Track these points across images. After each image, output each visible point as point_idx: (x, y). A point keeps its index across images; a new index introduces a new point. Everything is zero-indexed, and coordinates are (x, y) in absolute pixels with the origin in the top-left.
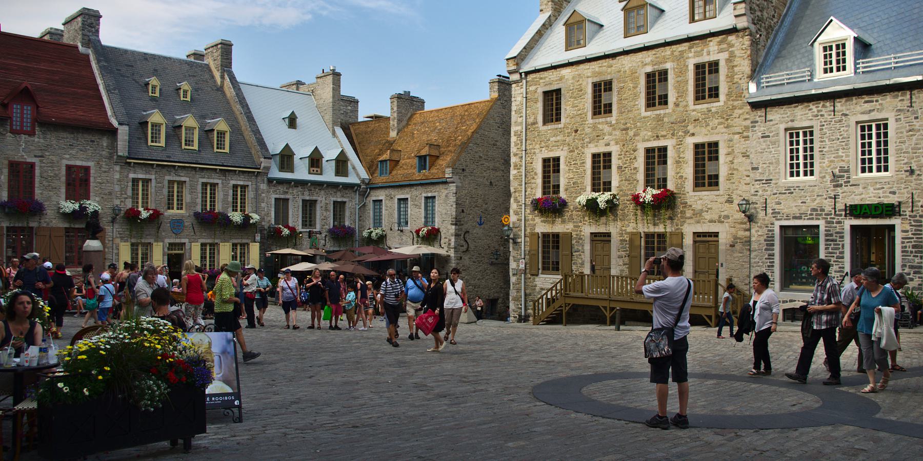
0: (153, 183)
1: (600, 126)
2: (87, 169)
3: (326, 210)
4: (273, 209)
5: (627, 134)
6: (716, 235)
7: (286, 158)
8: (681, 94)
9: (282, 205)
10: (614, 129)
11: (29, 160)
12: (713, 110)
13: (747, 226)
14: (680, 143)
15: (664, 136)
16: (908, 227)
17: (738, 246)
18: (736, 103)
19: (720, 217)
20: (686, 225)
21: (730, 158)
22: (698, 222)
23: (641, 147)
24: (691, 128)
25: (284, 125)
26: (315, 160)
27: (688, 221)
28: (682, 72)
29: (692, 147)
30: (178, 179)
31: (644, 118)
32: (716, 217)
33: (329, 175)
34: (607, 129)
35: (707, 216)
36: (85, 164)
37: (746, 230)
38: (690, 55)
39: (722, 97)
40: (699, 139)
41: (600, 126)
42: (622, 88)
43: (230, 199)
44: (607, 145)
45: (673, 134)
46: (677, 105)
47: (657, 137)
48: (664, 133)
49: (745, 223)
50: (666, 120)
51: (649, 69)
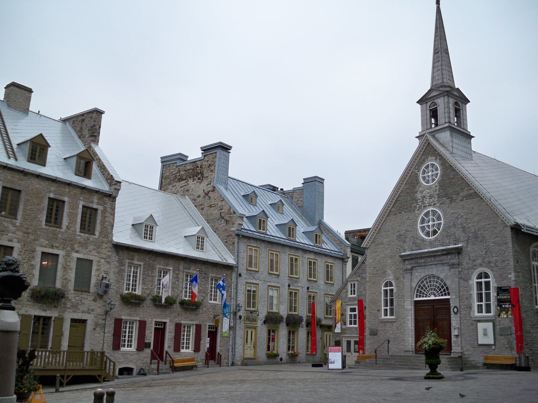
1: (6, 224)
5: (28, 237)
6: (84, 321)
8: (72, 221)
10: (18, 230)
12: (91, 239)
13: (104, 317)
14: (68, 255)
15: (57, 247)
17: (98, 329)
18: (104, 239)
19: (88, 310)
20: (66, 313)
21: (98, 273)
22: (75, 312)
23: (39, 250)
24: (76, 246)
27: (68, 310)
28: (74, 207)
29: (75, 259)
31: (44, 229)
32: (86, 309)
34: (11, 228)
35: (82, 308)
37: (103, 320)
38: (82, 198)
39: (97, 233)
40: (81, 256)
41: (6, 224)
42: (28, 200)
44: (11, 241)
45: (63, 248)
46: (68, 228)
47: (52, 246)
48: (57, 245)
49: (103, 315)
50: (59, 236)
51: (52, 196)
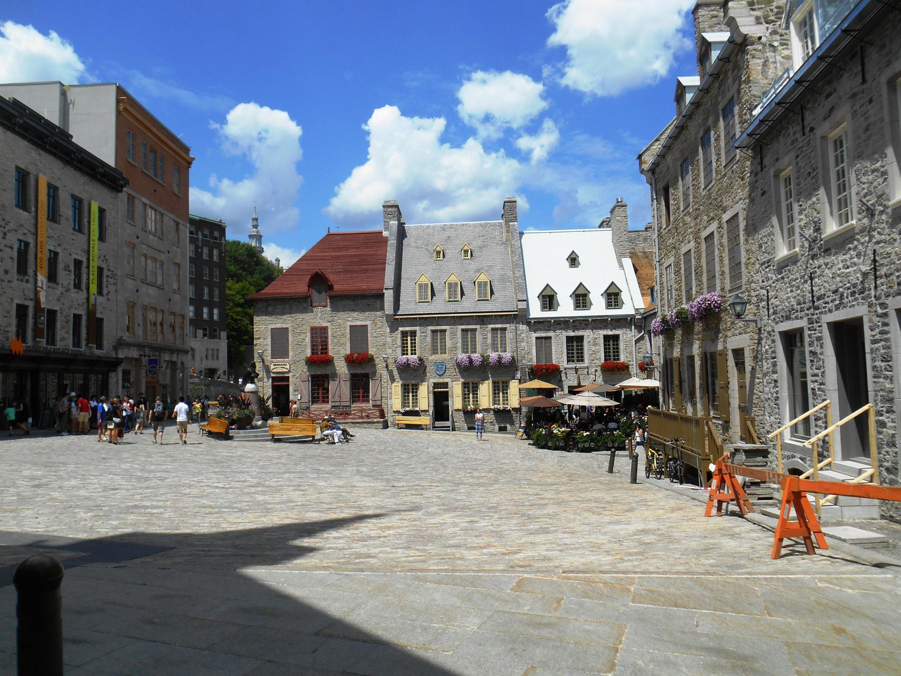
0: (418, 334)
2: (367, 326)
3: (595, 344)
4: (534, 348)
7: (549, 299)
9: (544, 343)
11: (324, 325)
16: (876, 319)
25: (567, 264)
26: (581, 298)
30: (439, 328)
33: (598, 308)
36: (363, 323)
43: (489, 341)
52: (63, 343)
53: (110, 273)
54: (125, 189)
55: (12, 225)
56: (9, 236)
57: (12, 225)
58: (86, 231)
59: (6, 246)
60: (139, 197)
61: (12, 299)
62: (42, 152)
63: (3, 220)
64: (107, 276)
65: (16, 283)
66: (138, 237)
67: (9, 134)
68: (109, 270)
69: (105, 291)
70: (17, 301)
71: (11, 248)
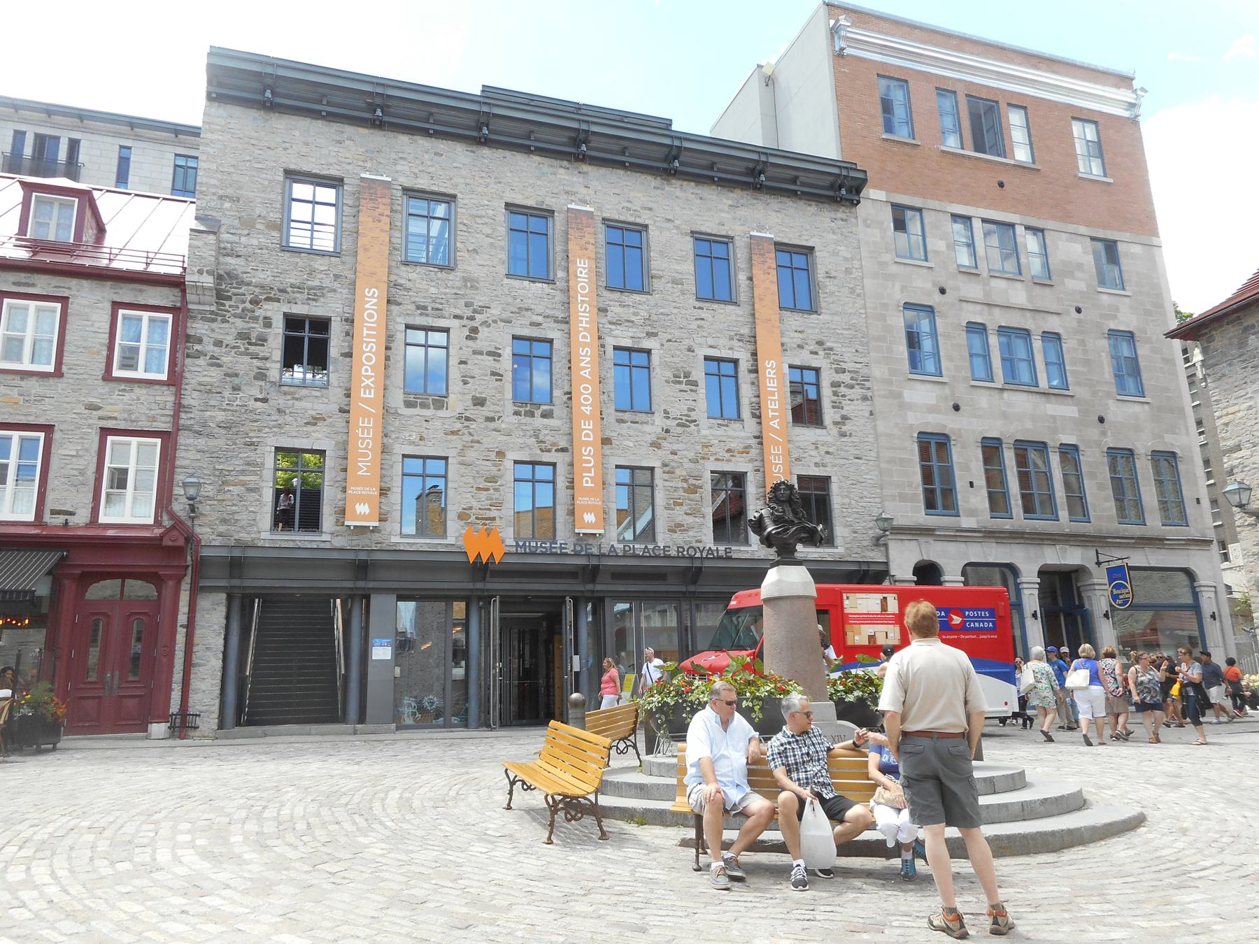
52: (679, 538)
53: (846, 378)
54: (872, 193)
55: (495, 311)
56: (484, 332)
57: (495, 311)
58: (743, 297)
59: (475, 352)
60: (931, 203)
61: (501, 454)
62: (585, 168)
63: (467, 305)
64: (835, 385)
65: (509, 420)
66: (943, 291)
67: (486, 151)
68: (838, 371)
69: (829, 415)
70: (512, 455)
71: (495, 354)
